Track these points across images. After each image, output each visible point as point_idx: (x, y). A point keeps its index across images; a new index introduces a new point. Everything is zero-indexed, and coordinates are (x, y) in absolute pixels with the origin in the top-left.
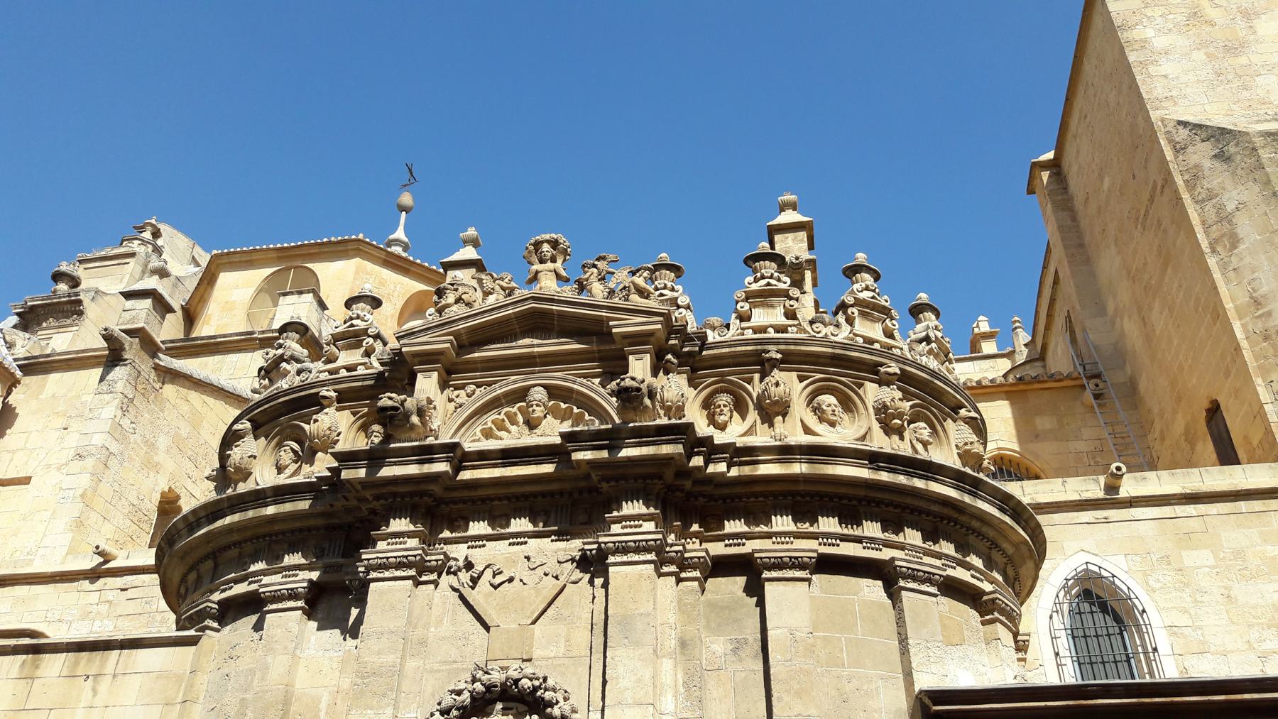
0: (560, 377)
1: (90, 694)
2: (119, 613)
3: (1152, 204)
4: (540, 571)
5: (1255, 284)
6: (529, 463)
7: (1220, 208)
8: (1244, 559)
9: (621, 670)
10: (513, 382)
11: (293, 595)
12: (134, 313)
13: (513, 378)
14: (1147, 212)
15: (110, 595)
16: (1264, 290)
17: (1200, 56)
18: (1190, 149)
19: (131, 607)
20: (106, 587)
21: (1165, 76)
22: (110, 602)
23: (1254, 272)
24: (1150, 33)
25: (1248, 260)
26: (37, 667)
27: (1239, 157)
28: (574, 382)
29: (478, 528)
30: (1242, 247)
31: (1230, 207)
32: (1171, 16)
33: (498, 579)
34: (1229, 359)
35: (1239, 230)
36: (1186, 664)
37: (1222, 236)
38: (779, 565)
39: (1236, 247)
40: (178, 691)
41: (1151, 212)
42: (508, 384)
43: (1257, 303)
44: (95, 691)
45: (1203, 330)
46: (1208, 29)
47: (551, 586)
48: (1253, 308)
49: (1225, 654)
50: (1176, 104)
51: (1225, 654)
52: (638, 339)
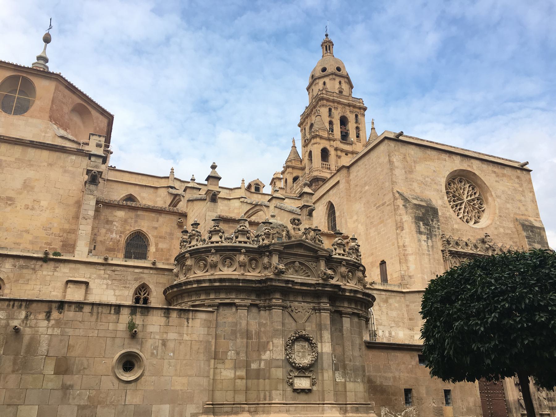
0: (302, 260)
1: (187, 323)
2: (113, 278)
3: (383, 206)
4: (305, 311)
5: (405, 242)
6: (305, 286)
7: (401, 219)
8: (391, 306)
9: (325, 335)
10: (292, 260)
11: (245, 306)
12: (96, 164)
13: (292, 258)
14: (379, 206)
15: (109, 272)
16: (406, 244)
17: (403, 171)
18: (398, 200)
19: (118, 278)
20: (107, 269)
21: (396, 175)
22: (109, 275)
23: (405, 239)
24: (395, 160)
25: (404, 235)
26: (169, 314)
27: (409, 208)
28: (306, 262)
29: (292, 299)
30: (404, 231)
31: (404, 220)
32: (400, 156)
33: (297, 311)
34: (393, 256)
35: (404, 227)
36: (378, 327)
37: (401, 227)
38: (346, 314)
39: (402, 231)
40: (211, 324)
41: (381, 207)
42: (291, 260)
43: (404, 246)
44: (188, 323)
45: (387, 245)
46: (406, 163)
47: (308, 314)
48: (403, 247)
49: (385, 326)
50: (397, 184)
51: (385, 326)
52: (322, 256)
